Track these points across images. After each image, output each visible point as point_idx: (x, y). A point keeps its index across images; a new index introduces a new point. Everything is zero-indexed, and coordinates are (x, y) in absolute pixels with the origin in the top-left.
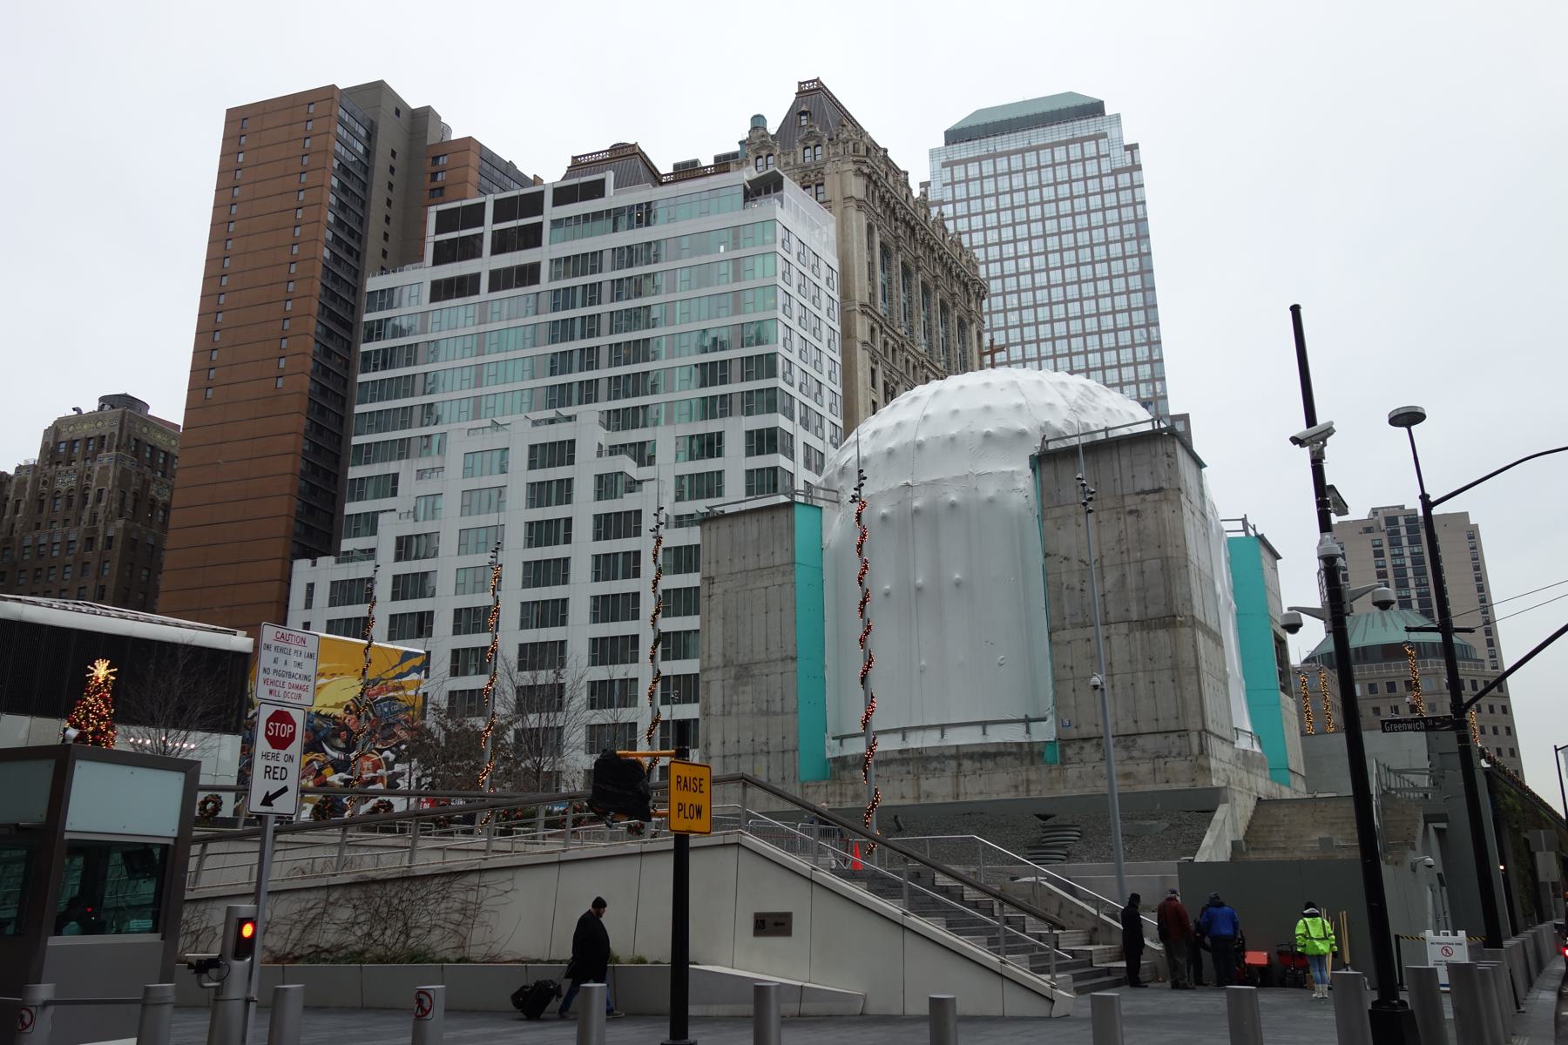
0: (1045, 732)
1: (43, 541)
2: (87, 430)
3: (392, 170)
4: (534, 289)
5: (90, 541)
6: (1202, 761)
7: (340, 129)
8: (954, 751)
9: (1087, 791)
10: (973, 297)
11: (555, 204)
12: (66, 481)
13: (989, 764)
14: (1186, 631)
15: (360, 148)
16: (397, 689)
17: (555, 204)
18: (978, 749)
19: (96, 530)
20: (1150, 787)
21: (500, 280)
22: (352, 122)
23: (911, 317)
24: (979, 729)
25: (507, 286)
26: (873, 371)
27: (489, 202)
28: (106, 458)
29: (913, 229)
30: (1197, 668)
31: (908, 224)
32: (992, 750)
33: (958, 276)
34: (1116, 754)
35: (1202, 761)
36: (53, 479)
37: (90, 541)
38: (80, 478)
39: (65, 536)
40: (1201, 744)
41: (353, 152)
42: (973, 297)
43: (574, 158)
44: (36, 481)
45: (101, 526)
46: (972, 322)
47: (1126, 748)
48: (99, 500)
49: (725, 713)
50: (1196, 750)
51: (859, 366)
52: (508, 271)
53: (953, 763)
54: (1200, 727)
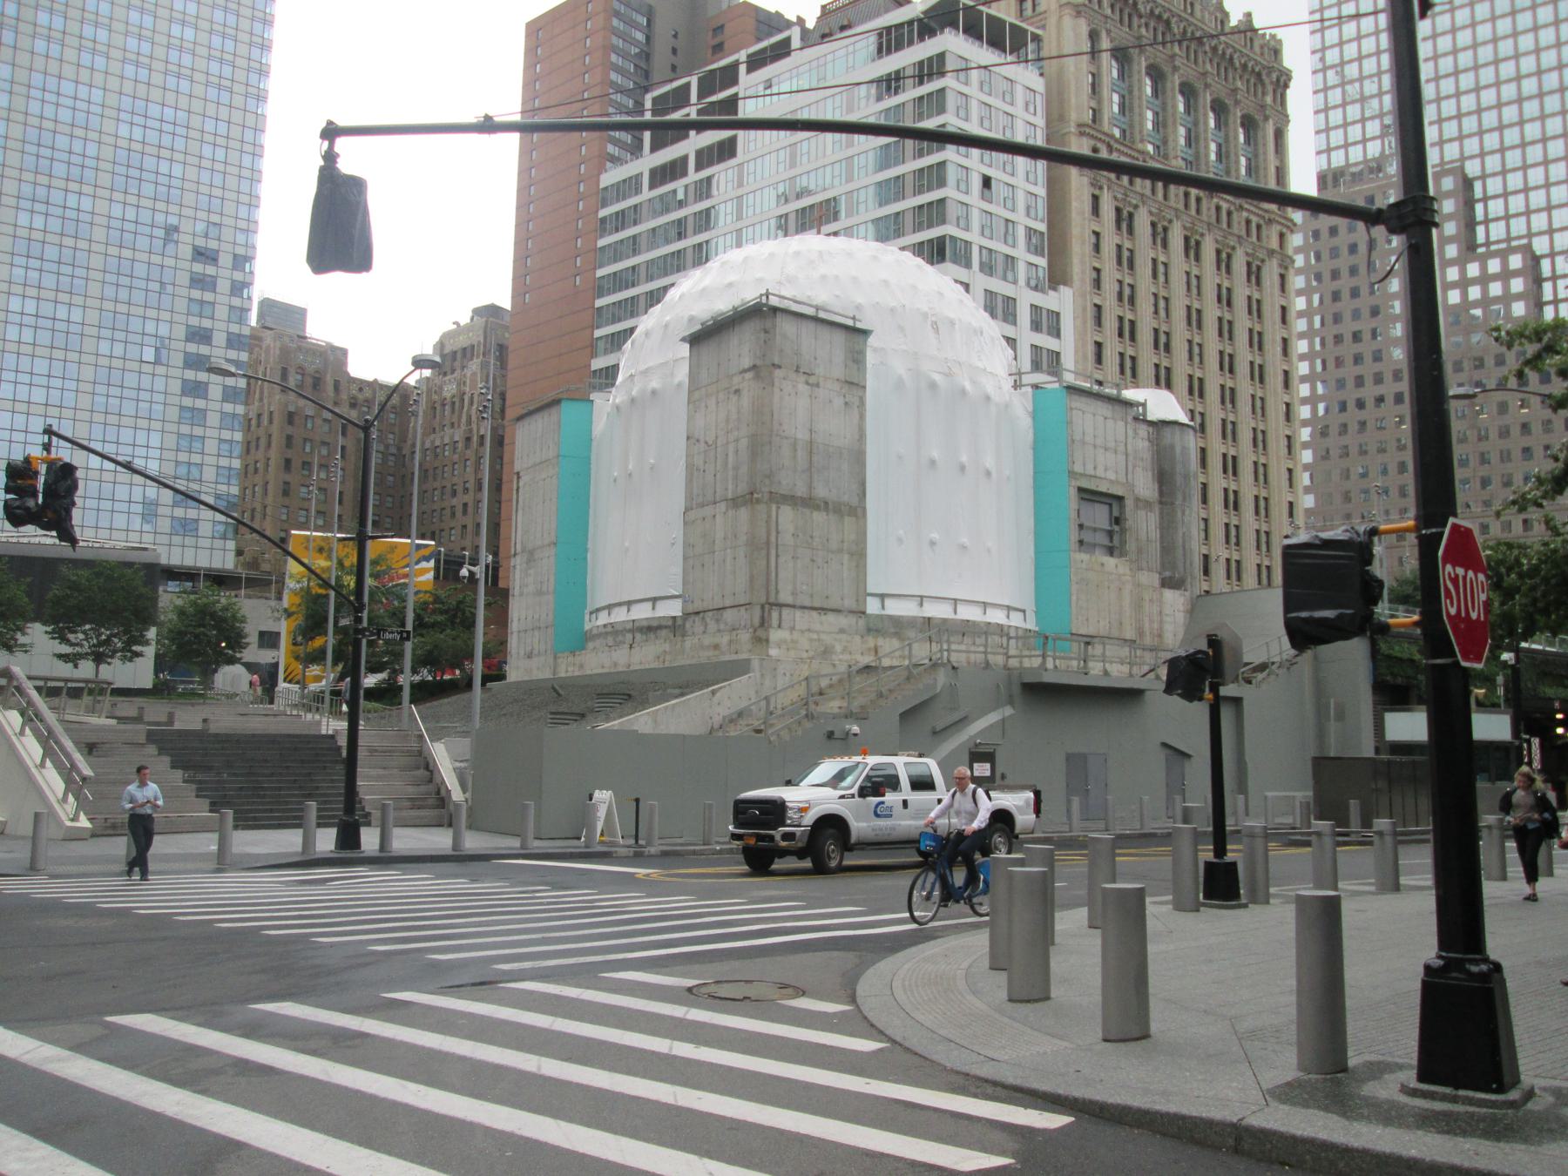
0: (673, 609)
1: (437, 443)
2: (462, 342)
3: (674, 51)
4: (733, 162)
5: (468, 439)
6: (760, 633)
7: (615, 22)
8: (629, 626)
9: (694, 661)
10: (1270, 88)
11: (749, 71)
12: (450, 390)
13: (652, 635)
14: (761, 508)
15: (640, 36)
16: (406, 576)
17: (749, 71)
18: (645, 624)
19: (471, 431)
20: (727, 658)
21: (707, 157)
22: (629, 11)
23: (1165, 126)
24: (649, 604)
25: (710, 164)
26: (1095, 198)
27: (694, 81)
28: (474, 365)
29: (1168, 23)
30: (768, 543)
31: (1159, 17)
32: (655, 624)
33: (1244, 66)
34: (712, 626)
35: (760, 633)
36: (441, 388)
37: (468, 439)
38: (459, 385)
39: (452, 437)
40: (762, 618)
41: (635, 43)
42: (1270, 88)
43: (823, 7)
44: (429, 391)
45: (474, 426)
46: (1266, 118)
47: (717, 621)
48: (471, 403)
49: (521, 594)
50: (757, 621)
51: (1074, 194)
52: (710, 148)
53: (629, 636)
54: (763, 600)
